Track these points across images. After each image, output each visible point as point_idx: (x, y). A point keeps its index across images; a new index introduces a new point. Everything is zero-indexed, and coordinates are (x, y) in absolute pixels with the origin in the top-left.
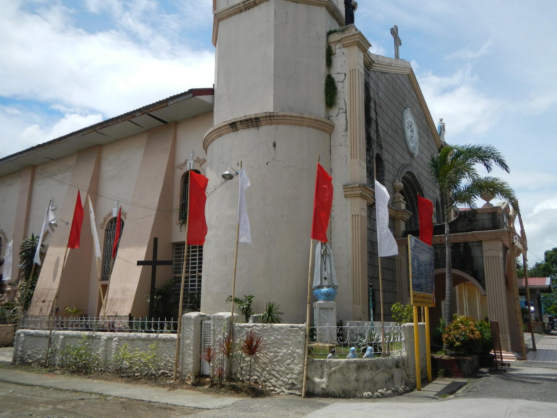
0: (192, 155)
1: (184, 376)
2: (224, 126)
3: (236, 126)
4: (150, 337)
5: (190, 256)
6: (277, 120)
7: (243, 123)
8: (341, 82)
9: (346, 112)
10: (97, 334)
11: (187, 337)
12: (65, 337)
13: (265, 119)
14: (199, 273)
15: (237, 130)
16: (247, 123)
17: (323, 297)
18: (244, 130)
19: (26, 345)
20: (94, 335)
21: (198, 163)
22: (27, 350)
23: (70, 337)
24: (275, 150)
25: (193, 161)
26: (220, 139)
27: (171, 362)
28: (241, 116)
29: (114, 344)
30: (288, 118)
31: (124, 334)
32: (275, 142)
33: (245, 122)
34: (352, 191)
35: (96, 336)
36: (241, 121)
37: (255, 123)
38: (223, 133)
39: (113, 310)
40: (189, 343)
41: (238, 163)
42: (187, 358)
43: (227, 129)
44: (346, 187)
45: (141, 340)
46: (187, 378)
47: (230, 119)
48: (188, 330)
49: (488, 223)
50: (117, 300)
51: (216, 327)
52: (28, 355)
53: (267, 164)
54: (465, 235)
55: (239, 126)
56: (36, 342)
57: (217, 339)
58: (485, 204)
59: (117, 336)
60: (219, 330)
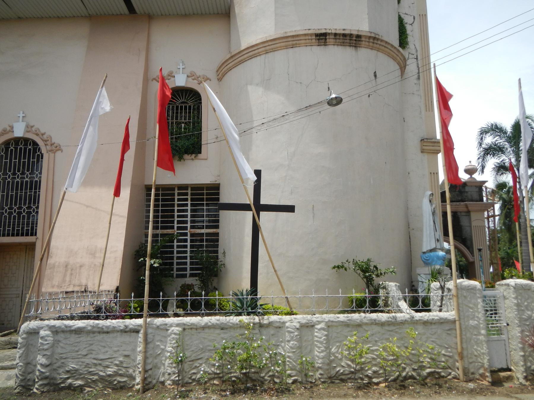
0: (184, 67)
1: (473, 373)
2: (305, 35)
3: (326, 39)
4: (398, 319)
5: (176, 205)
6: (380, 45)
7: (338, 37)
8: (410, 24)
9: (417, 59)
10: (271, 320)
11: (471, 317)
12: (184, 329)
13: (367, 40)
14: (192, 230)
15: (324, 45)
16: (343, 39)
17: (440, 262)
18: (336, 46)
19: (59, 350)
20: (266, 322)
21: (193, 80)
22: (63, 361)
23: (196, 329)
24: (376, 81)
25: (186, 75)
26: (291, 51)
27: (444, 355)
28: (338, 28)
29: (319, 335)
30: (389, 47)
31: (338, 318)
32: (375, 72)
33: (341, 37)
34: (433, 146)
35: (270, 324)
36: (336, 34)
37: (354, 42)
38: (299, 44)
39: (77, 282)
40: (477, 324)
41: (329, 88)
42: (475, 347)
43: (309, 39)
44: (429, 141)
45: (376, 324)
46: (477, 376)
47: (316, 27)
48: (471, 305)
49: (476, 196)
50: (81, 266)
51: (521, 300)
52: (68, 372)
53: (369, 96)
54: (458, 205)
55: (332, 40)
56: (92, 344)
57: (524, 317)
58: (469, 178)
59: (322, 322)
60: (526, 303)
